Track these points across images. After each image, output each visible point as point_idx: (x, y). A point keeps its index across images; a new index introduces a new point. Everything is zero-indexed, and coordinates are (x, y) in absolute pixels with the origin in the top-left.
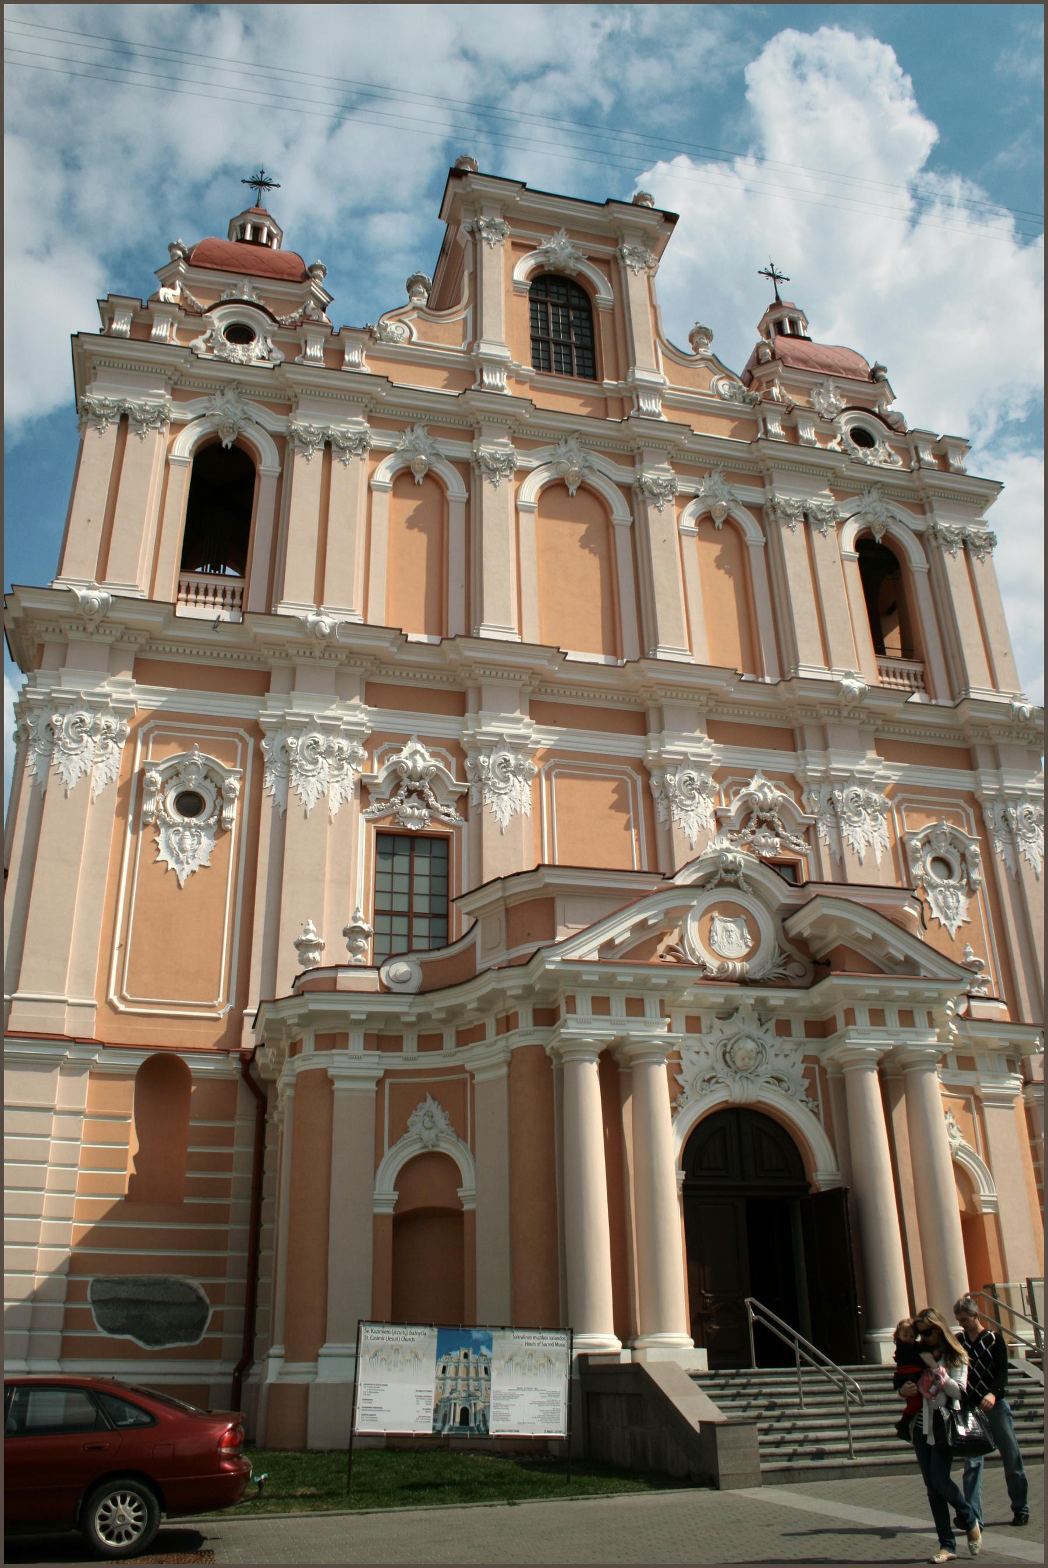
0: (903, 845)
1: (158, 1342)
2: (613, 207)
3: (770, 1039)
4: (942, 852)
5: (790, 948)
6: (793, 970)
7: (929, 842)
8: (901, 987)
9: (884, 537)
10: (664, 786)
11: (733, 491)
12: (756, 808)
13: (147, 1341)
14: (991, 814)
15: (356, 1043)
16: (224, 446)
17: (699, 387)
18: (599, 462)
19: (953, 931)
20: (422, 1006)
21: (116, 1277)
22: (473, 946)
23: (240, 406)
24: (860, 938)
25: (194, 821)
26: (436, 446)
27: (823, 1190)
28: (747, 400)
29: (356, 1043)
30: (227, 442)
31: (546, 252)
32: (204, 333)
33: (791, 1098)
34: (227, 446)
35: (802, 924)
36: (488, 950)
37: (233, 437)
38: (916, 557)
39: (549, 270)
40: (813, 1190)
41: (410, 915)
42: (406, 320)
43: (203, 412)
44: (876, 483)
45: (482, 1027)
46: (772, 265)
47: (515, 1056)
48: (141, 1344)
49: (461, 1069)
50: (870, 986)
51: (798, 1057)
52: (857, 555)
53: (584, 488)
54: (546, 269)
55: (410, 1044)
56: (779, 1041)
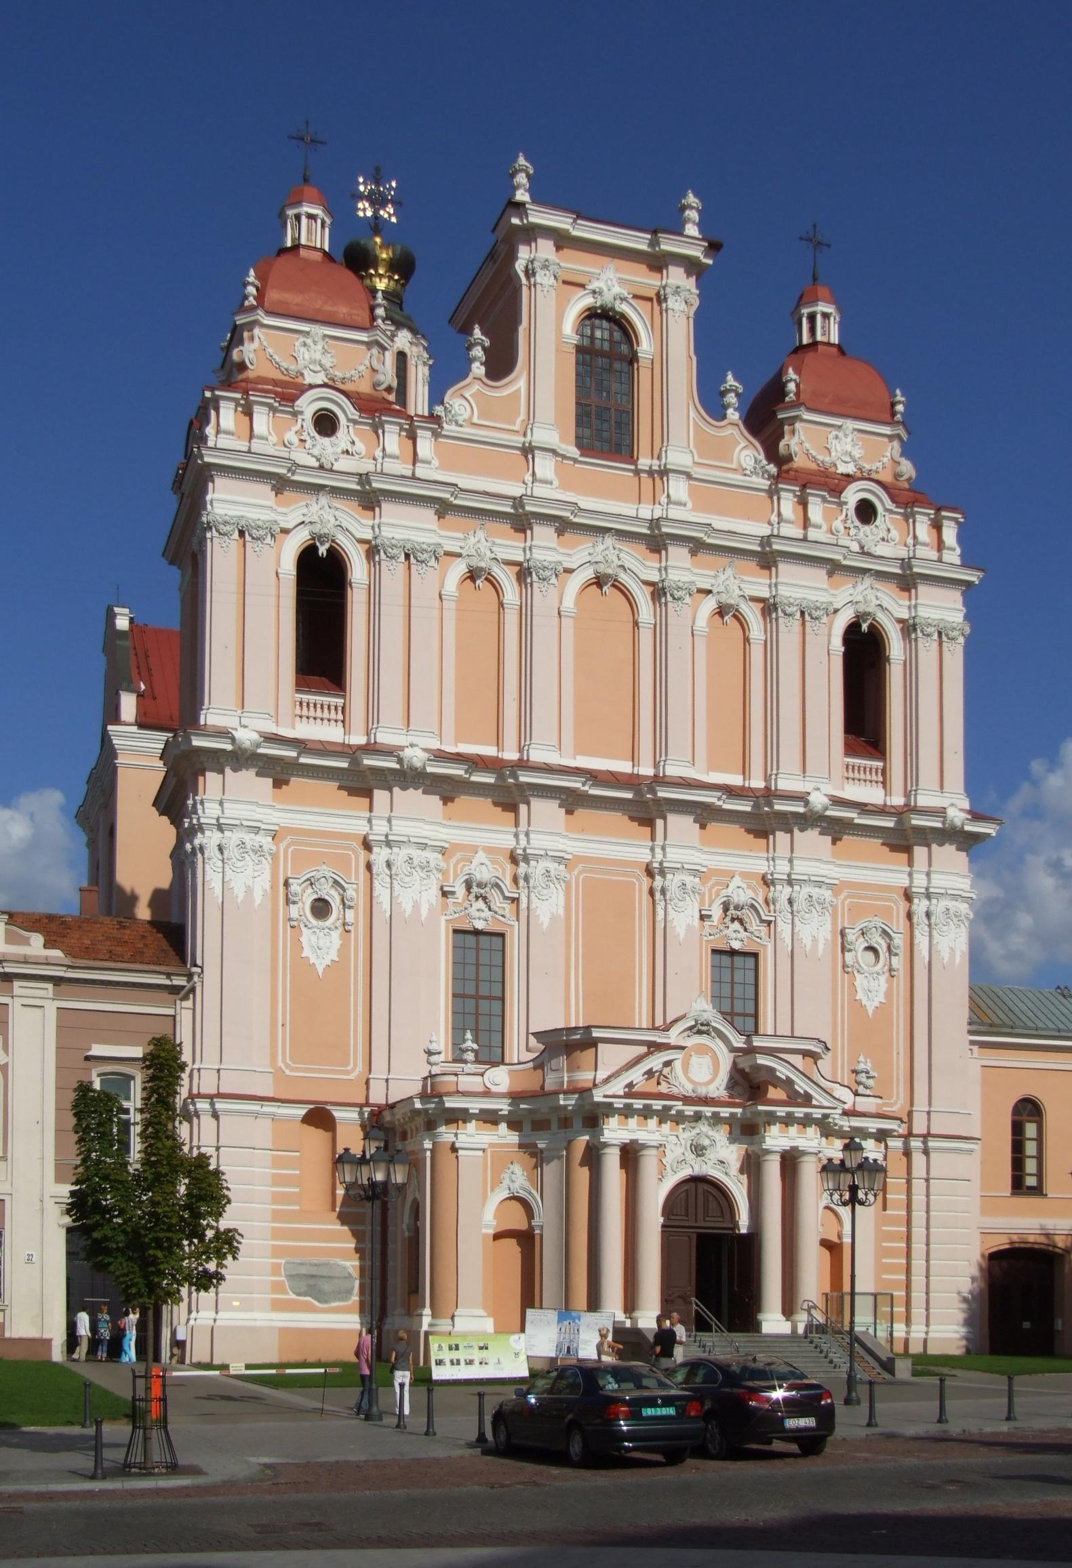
0: (843, 934)
7: (863, 934)
9: (871, 626)
10: (663, 891)
11: (742, 586)
12: (732, 907)
14: (920, 906)
19: (870, 1012)
23: (332, 511)
25: (321, 923)
26: (493, 549)
28: (766, 476)
42: (467, 395)
43: (301, 519)
44: (870, 570)
52: (843, 649)
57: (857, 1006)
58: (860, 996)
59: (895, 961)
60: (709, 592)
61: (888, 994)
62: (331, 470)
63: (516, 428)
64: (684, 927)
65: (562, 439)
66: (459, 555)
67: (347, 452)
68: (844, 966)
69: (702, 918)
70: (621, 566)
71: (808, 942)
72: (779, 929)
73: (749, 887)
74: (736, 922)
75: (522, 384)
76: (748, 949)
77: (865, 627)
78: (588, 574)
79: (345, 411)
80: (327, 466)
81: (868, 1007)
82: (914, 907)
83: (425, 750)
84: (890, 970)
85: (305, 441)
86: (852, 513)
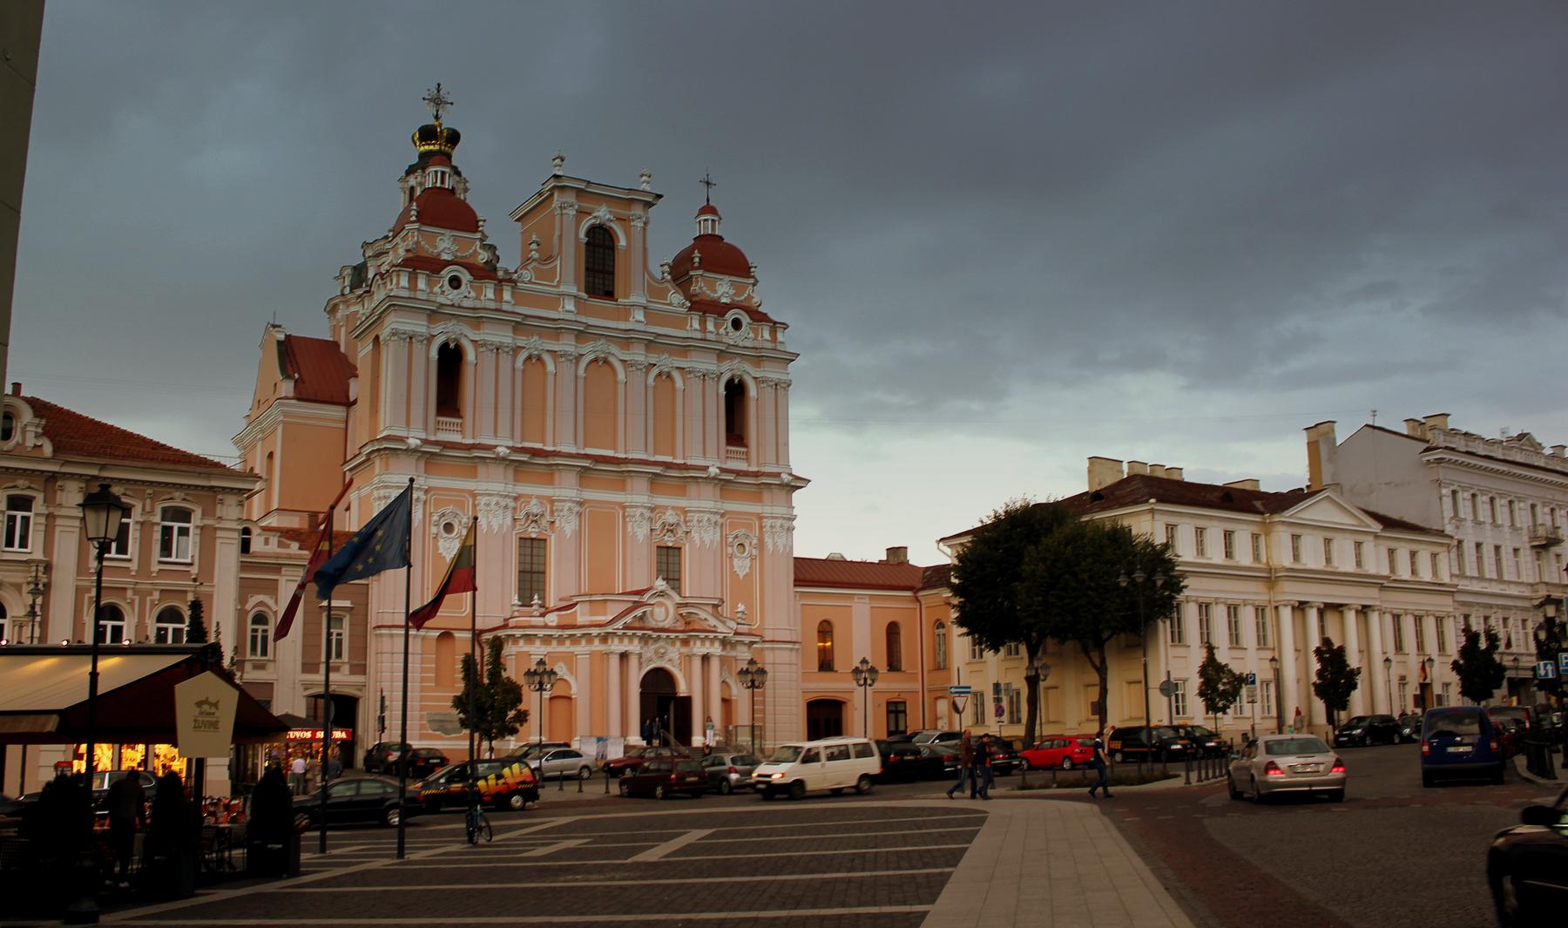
1: (448, 734)
3: (670, 648)
5: (679, 617)
6: (679, 624)
8: (712, 635)
13: (446, 734)
14: (767, 523)
15: (538, 643)
18: (614, 349)
19: (741, 577)
20: (560, 632)
21: (433, 712)
22: (576, 611)
24: (701, 619)
27: (682, 695)
29: (538, 643)
31: (595, 217)
32: (439, 283)
33: (674, 667)
35: (684, 611)
36: (583, 614)
40: (678, 695)
41: (532, 572)
45: (580, 641)
46: (708, 175)
47: (592, 654)
48: (443, 735)
49: (573, 652)
50: (702, 635)
51: (677, 653)
53: (606, 361)
55: (554, 643)
56: (671, 648)
57: (734, 574)
60: (655, 365)
61: (751, 568)
62: (459, 307)
63: (555, 284)
65: (579, 291)
66: (524, 348)
67: (465, 297)
69: (652, 530)
70: (609, 353)
73: (676, 514)
75: (558, 262)
77: (736, 381)
78: (592, 356)
79: (466, 277)
80: (456, 305)
82: (764, 524)
83: (507, 447)
85: (444, 291)
86: (730, 324)
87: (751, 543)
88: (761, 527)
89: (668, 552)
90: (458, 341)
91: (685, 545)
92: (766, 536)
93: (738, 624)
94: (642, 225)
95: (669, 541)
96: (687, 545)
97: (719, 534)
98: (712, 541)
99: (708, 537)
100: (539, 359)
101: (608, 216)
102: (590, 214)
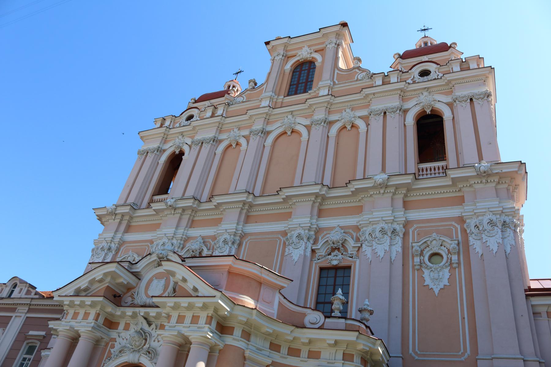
2: (322, 30)
4: (435, 250)
16: (176, 153)
17: (348, 80)
19: (436, 291)
30: (177, 152)
34: (177, 153)
37: (179, 150)
38: (447, 115)
39: (302, 61)
54: (300, 61)
58: (428, 282)
59: (455, 258)
61: (451, 279)
64: (298, 256)
68: (414, 266)
69: (313, 251)
71: (381, 254)
72: (364, 250)
74: (336, 251)
76: (343, 264)
81: (434, 290)
84: (451, 264)
87: (448, 250)
88: (464, 231)
89: (336, 273)
90: (181, 148)
91: (355, 262)
92: (470, 239)
93: (326, 317)
94: (334, 45)
95: (335, 260)
96: (358, 262)
97: (400, 244)
98: (388, 252)
99: (381, 250)
100: (238, 144)
101: (309, 51)
102: (296, 56)
